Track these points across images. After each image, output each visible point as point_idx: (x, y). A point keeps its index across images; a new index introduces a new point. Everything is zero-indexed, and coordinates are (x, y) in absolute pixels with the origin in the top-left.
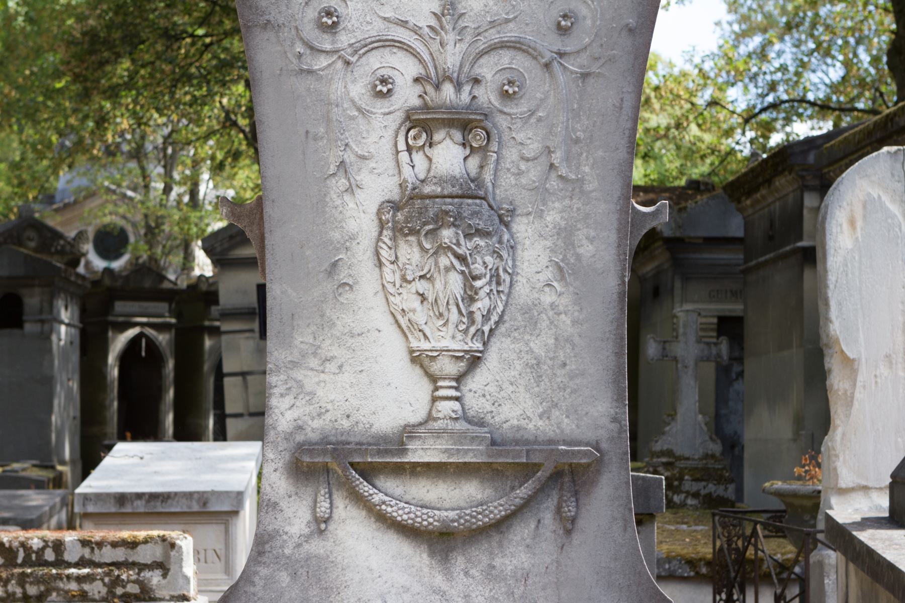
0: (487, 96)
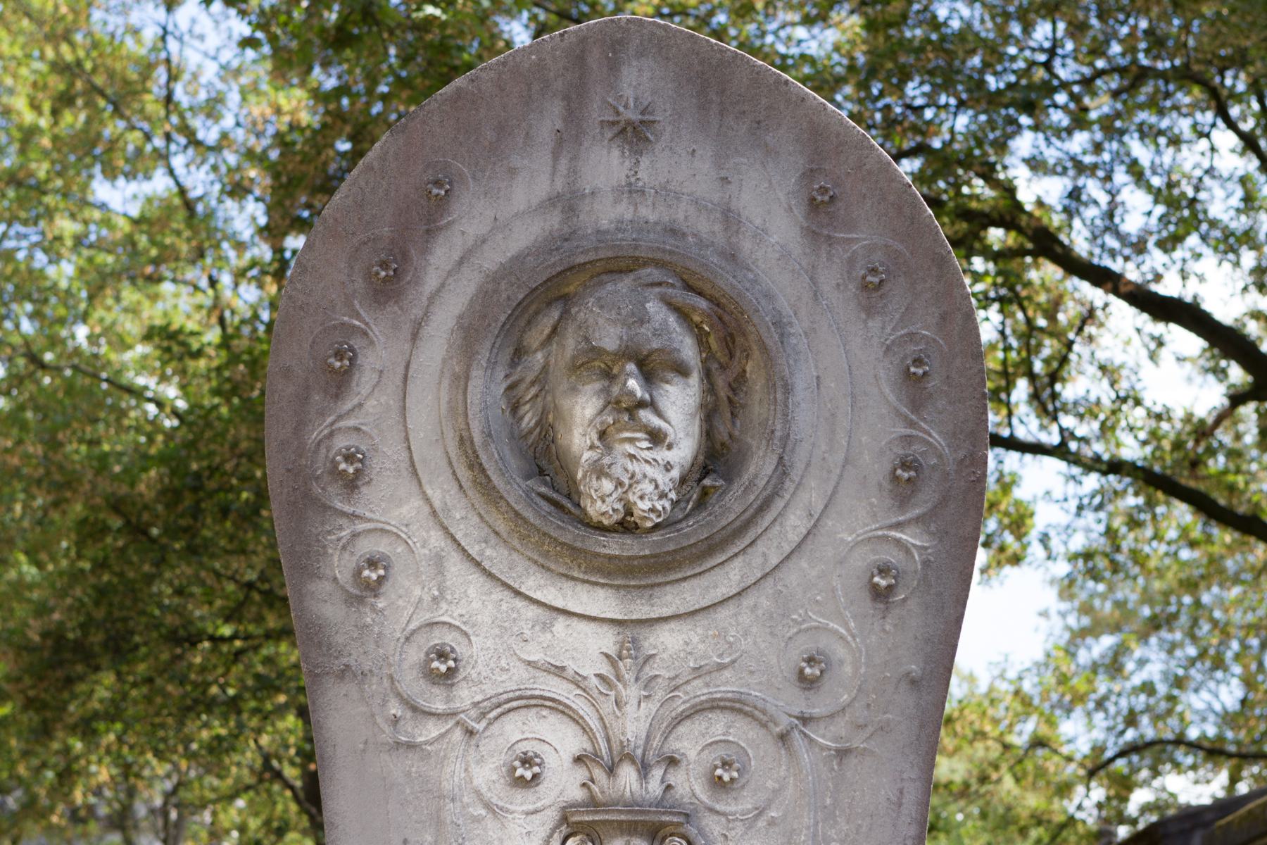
0: (689, 784)
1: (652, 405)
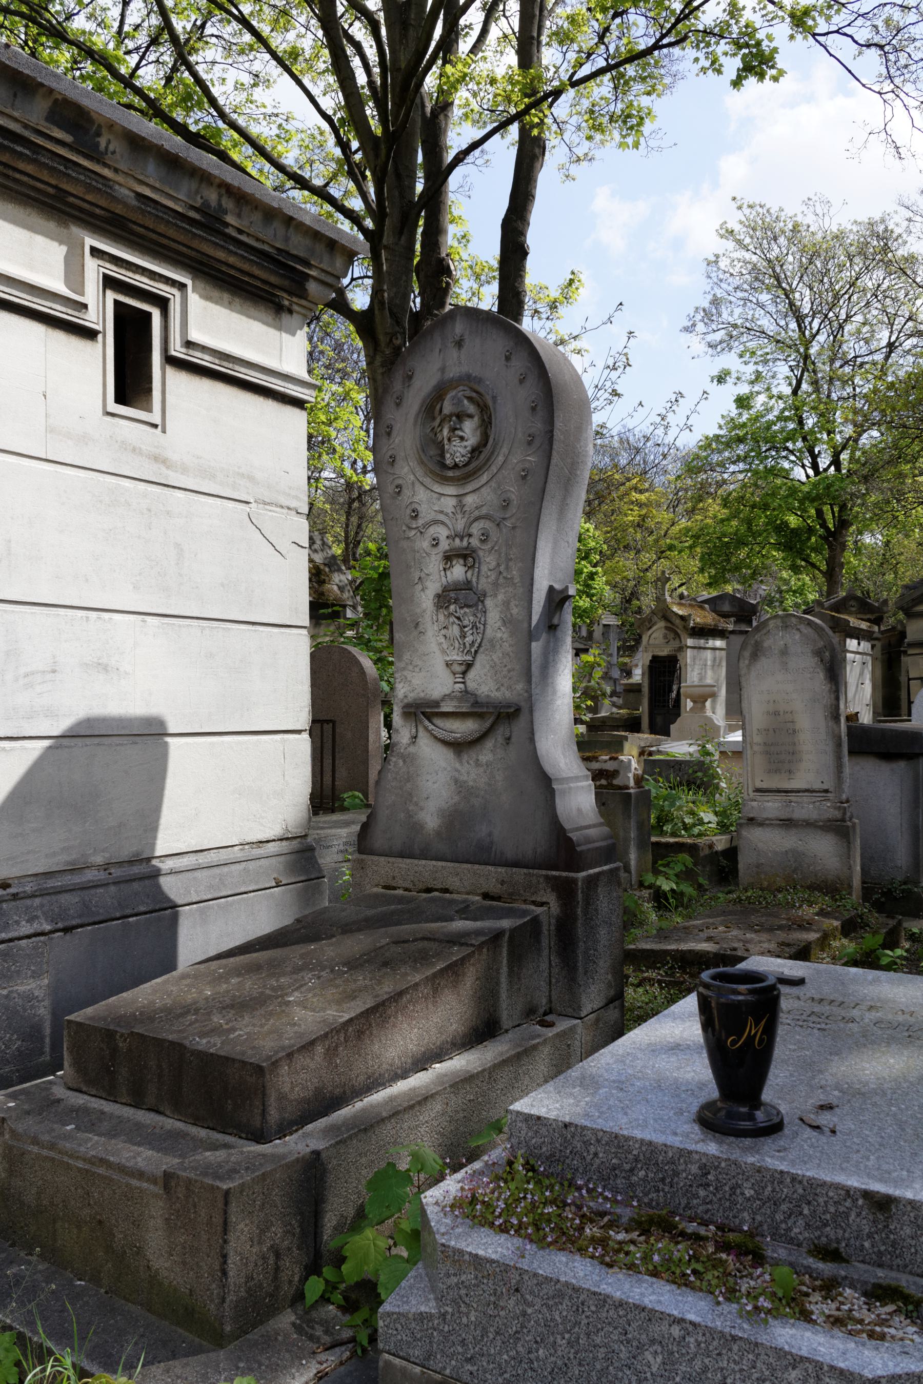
0: (475, 542)
1: (461, 429)
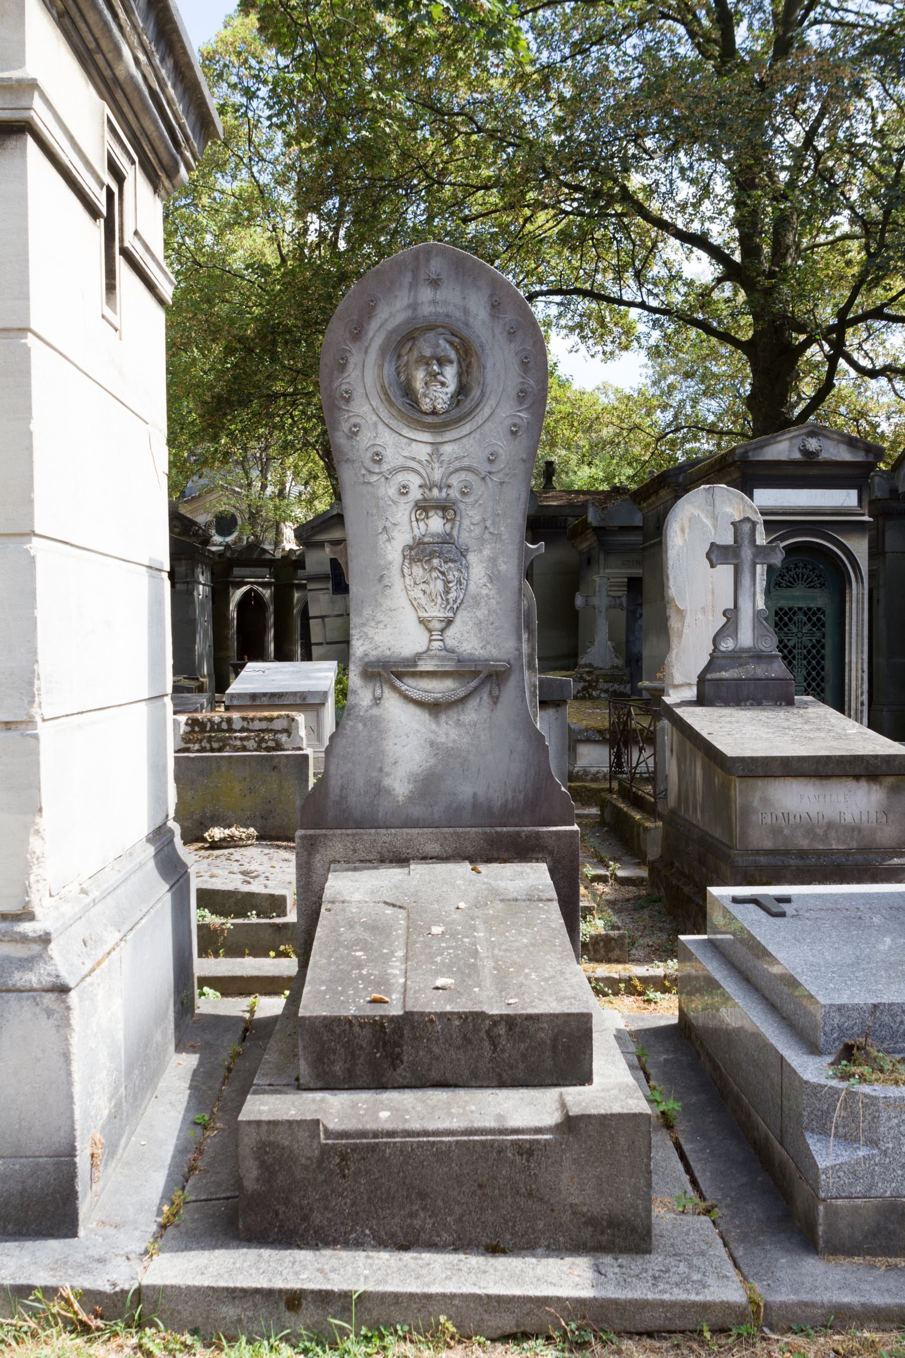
0: (454, 493)
1: (441, 374)
